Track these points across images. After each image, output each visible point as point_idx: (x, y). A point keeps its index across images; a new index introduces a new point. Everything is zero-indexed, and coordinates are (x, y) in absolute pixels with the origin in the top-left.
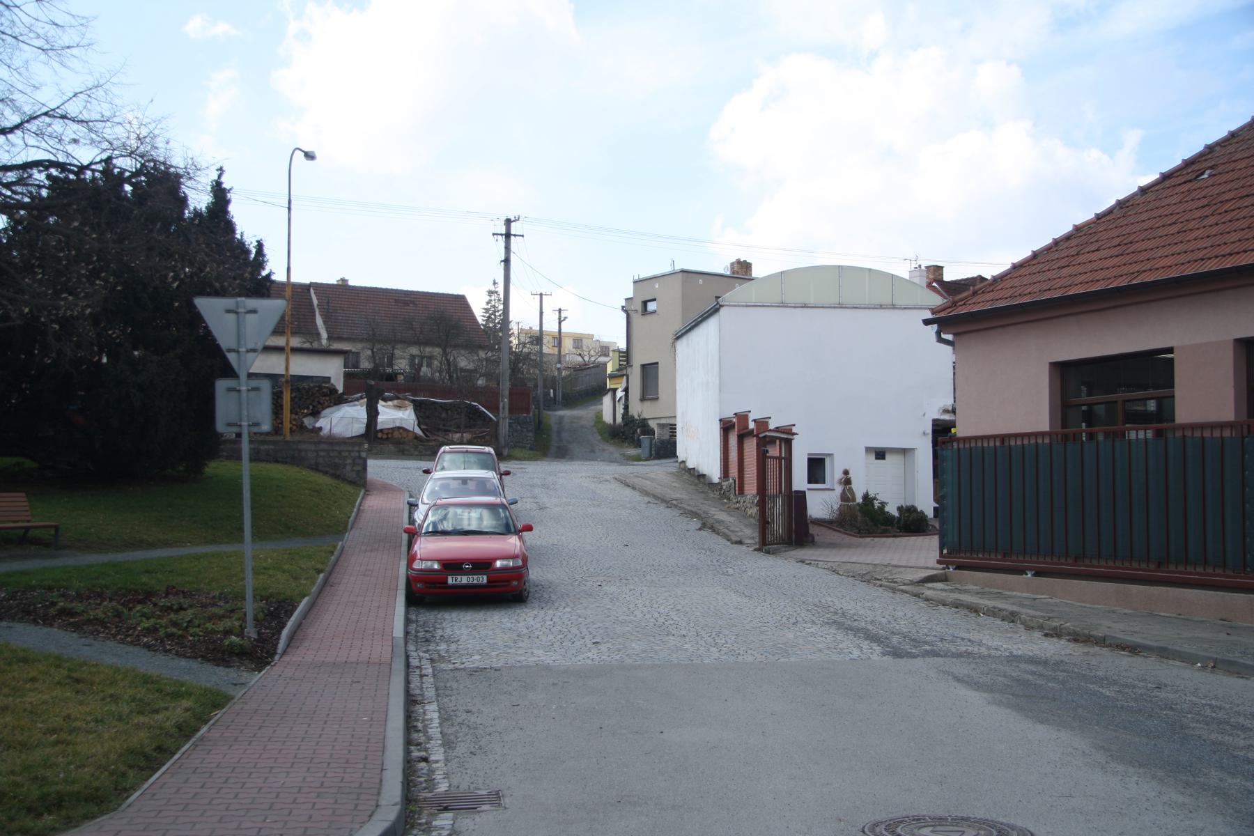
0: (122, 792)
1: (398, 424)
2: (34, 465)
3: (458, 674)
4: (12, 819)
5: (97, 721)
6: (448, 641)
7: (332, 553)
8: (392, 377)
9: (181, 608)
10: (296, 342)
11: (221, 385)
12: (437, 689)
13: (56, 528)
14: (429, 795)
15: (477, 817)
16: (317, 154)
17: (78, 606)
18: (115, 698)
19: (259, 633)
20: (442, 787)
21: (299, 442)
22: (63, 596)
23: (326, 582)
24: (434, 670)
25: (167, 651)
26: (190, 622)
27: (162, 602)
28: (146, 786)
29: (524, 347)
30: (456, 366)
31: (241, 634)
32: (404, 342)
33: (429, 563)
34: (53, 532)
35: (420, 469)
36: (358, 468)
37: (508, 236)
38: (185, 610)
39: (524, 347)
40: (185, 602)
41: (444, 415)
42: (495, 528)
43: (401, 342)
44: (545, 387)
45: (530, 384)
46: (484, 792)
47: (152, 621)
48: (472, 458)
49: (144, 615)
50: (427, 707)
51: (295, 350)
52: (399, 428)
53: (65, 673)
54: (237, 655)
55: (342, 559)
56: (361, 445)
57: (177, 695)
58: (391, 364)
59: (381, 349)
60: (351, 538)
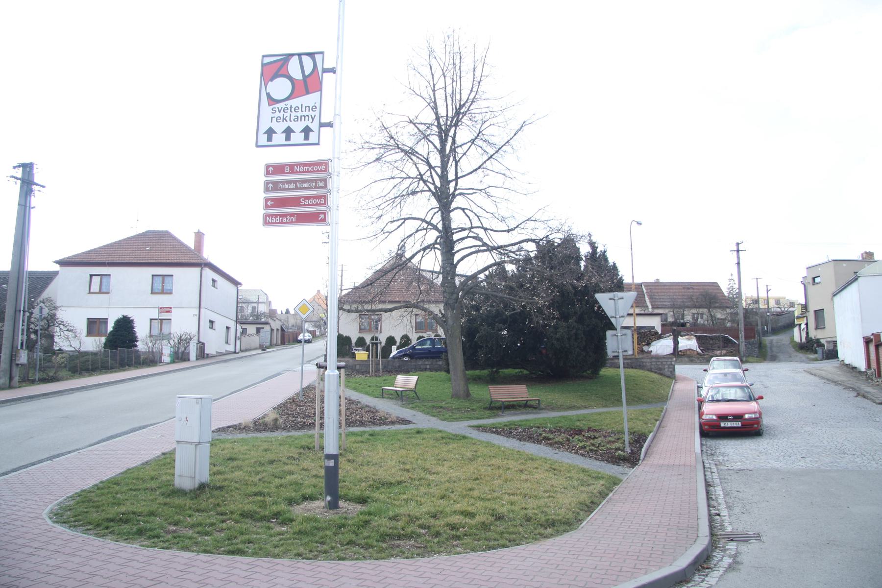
0: (579, 521)
1: (689, 348)
2: (528, 372)
3: (730, 472)
4: (535, 529)
5: (564, 488)
6: (723, 455)
7: (662, 411)
8: (684, 325)
9: (595, 438)
10: (638, 311)
11: (609, 333)
12: (720, 479)
13: (539, 400)
14: (723, 533)
15: (749, 545)
16: (642, 222)
17: (551, 436)
18: (571, 478)
19: (631, 450)
20: (729, 529)
21: (643, 358)
22: (544, 431)
23: (660, 424)
24: (717, 470)
25: (590, 457)
26: (599, 444)
27: (587, 434)
28: (588, 519)
29: (749, 305)
30: (715, 317)
31: (623, 450)
32: (689, 307)
33: (711, 416)
34: (537, 402)
35: (701, 369)
36: (671, 370)
37: (738, 251)
38: (597, 438)
39: (749, 305)
40: (597, 434)
41: (711, 342)
42: (743, 397)
43: (687, 307)
44: (762, 325)
45: (754, 324)
46: (752, 533)
47: (583, 443)
48: (728, 363)
49: (579, 440)
50: (716, 488)
51: (637, 315)
52: (689, 349)
53: (549, 466)
54: (622, 460)
55: (666, 414)
56: (672, 358)
57: (597, 478)
58: (683, 318)
59: (677, 312)
60: (670, 404)
